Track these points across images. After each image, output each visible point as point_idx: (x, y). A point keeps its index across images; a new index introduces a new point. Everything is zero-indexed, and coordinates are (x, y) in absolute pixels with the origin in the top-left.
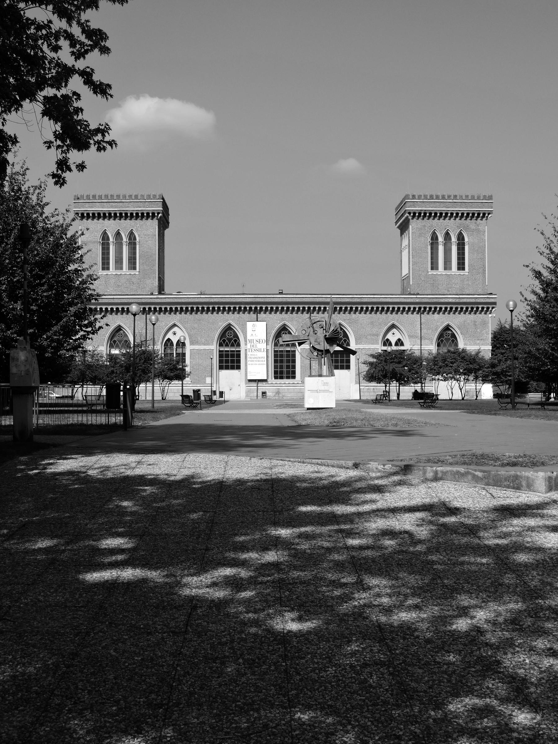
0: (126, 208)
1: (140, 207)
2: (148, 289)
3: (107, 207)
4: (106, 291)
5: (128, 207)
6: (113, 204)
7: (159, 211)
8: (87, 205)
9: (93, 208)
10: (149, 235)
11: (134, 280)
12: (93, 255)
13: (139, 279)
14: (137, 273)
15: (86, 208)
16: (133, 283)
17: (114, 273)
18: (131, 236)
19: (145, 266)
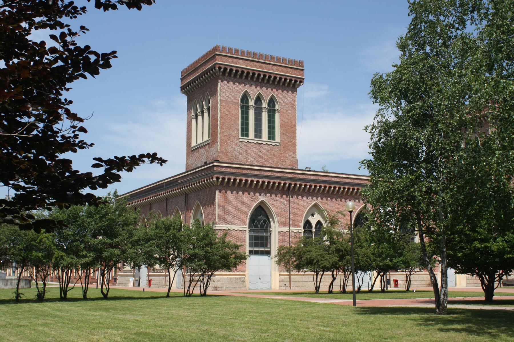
0: (269, 69)
1: (283, 72)
2: (288, 163)
3: (251, 66)
4: (247, 161)
5: (272, 69)
6: (258, 64)
7: (302, 80)
8: (230, 60)
9: (236, 63)
10: (288, 104)
11: (274, 151)
12: (233, 118)
13: (279, 151)
14: (278, 144)
15: (229, 62)
16: (274, 155)
17: (255, 142)
18: (272, 102)
19: (286, 138)
